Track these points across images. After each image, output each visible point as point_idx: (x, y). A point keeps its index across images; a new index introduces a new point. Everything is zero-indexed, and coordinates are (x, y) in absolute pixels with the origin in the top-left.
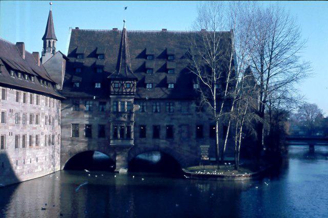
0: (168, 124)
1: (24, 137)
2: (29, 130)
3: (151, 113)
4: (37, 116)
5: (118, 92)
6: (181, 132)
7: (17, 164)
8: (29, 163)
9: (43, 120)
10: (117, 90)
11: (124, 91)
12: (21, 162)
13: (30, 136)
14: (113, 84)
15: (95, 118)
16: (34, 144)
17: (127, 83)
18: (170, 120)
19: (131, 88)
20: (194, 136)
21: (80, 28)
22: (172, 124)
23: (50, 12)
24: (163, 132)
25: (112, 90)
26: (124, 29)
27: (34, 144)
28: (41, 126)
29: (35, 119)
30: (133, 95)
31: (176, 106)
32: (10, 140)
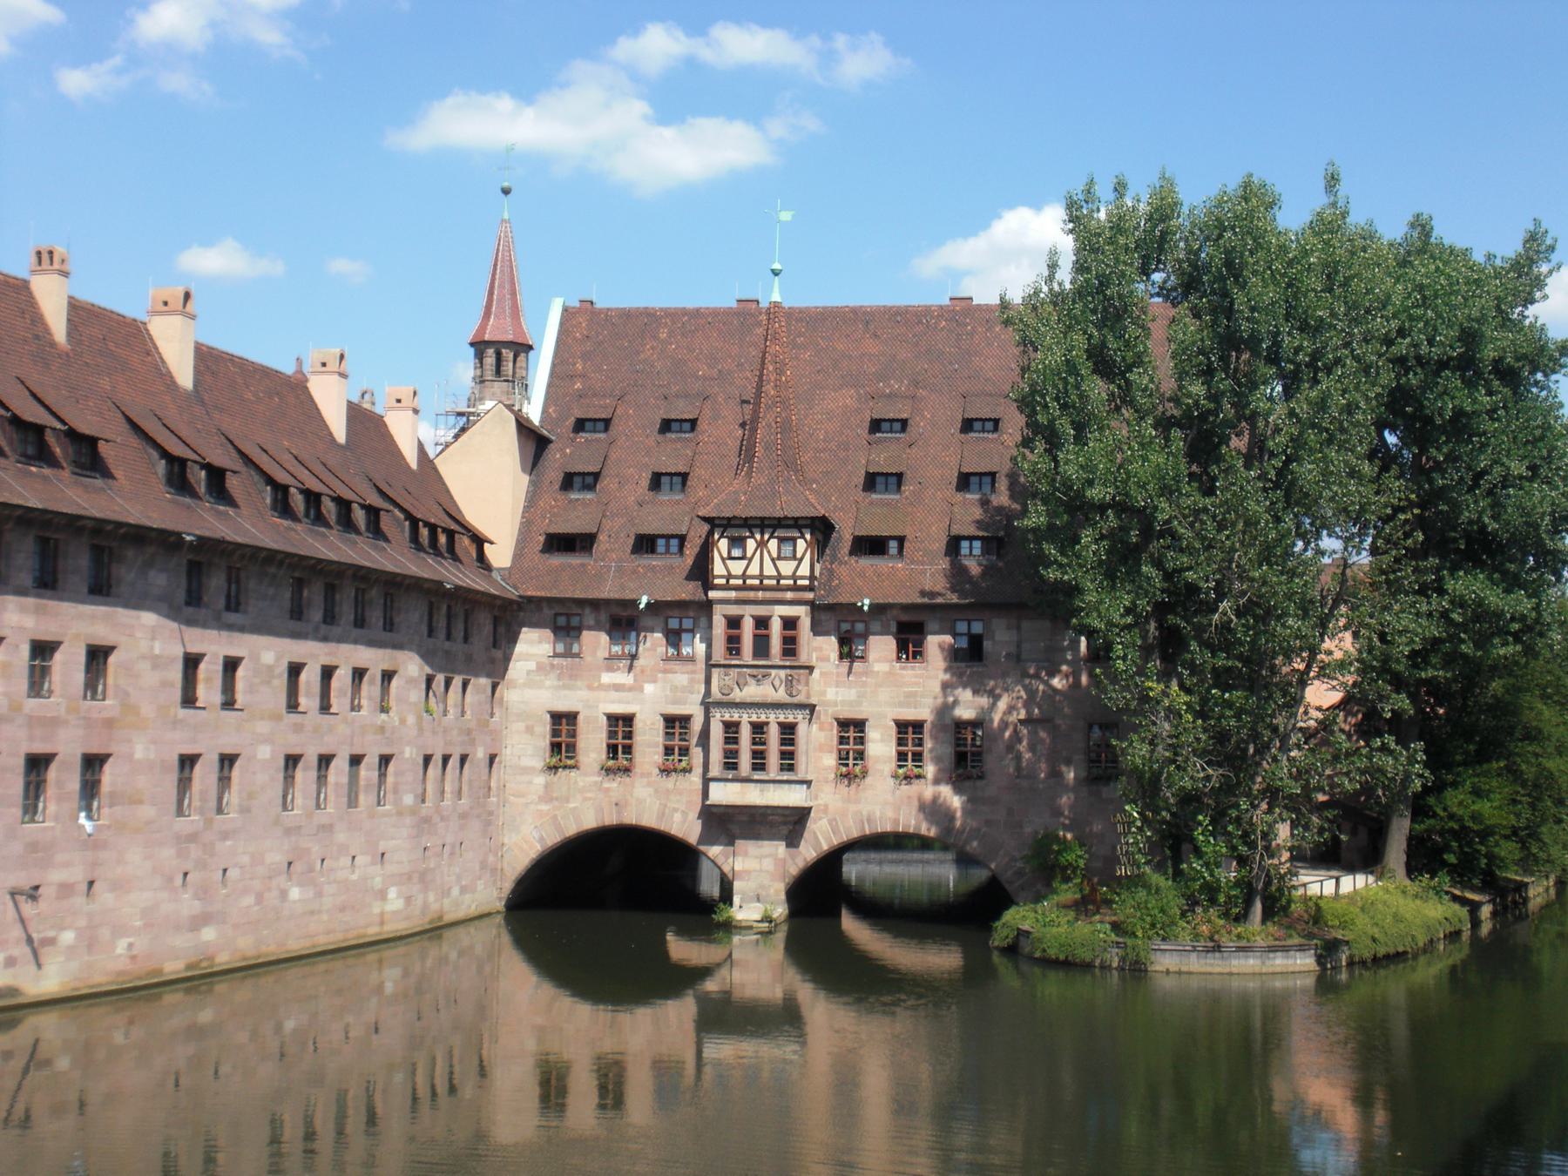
1: (325, 761)
5: (744, 576)
11: (769, 570)
12: (311, 870)
13: (356, 760)
14: (723, 544)
15: (649, 688)
19: (801, 560)
21: (600, 304)
25: (718, 568)
28: (403, 721)
30: (810, 588)
31: (998, 637)
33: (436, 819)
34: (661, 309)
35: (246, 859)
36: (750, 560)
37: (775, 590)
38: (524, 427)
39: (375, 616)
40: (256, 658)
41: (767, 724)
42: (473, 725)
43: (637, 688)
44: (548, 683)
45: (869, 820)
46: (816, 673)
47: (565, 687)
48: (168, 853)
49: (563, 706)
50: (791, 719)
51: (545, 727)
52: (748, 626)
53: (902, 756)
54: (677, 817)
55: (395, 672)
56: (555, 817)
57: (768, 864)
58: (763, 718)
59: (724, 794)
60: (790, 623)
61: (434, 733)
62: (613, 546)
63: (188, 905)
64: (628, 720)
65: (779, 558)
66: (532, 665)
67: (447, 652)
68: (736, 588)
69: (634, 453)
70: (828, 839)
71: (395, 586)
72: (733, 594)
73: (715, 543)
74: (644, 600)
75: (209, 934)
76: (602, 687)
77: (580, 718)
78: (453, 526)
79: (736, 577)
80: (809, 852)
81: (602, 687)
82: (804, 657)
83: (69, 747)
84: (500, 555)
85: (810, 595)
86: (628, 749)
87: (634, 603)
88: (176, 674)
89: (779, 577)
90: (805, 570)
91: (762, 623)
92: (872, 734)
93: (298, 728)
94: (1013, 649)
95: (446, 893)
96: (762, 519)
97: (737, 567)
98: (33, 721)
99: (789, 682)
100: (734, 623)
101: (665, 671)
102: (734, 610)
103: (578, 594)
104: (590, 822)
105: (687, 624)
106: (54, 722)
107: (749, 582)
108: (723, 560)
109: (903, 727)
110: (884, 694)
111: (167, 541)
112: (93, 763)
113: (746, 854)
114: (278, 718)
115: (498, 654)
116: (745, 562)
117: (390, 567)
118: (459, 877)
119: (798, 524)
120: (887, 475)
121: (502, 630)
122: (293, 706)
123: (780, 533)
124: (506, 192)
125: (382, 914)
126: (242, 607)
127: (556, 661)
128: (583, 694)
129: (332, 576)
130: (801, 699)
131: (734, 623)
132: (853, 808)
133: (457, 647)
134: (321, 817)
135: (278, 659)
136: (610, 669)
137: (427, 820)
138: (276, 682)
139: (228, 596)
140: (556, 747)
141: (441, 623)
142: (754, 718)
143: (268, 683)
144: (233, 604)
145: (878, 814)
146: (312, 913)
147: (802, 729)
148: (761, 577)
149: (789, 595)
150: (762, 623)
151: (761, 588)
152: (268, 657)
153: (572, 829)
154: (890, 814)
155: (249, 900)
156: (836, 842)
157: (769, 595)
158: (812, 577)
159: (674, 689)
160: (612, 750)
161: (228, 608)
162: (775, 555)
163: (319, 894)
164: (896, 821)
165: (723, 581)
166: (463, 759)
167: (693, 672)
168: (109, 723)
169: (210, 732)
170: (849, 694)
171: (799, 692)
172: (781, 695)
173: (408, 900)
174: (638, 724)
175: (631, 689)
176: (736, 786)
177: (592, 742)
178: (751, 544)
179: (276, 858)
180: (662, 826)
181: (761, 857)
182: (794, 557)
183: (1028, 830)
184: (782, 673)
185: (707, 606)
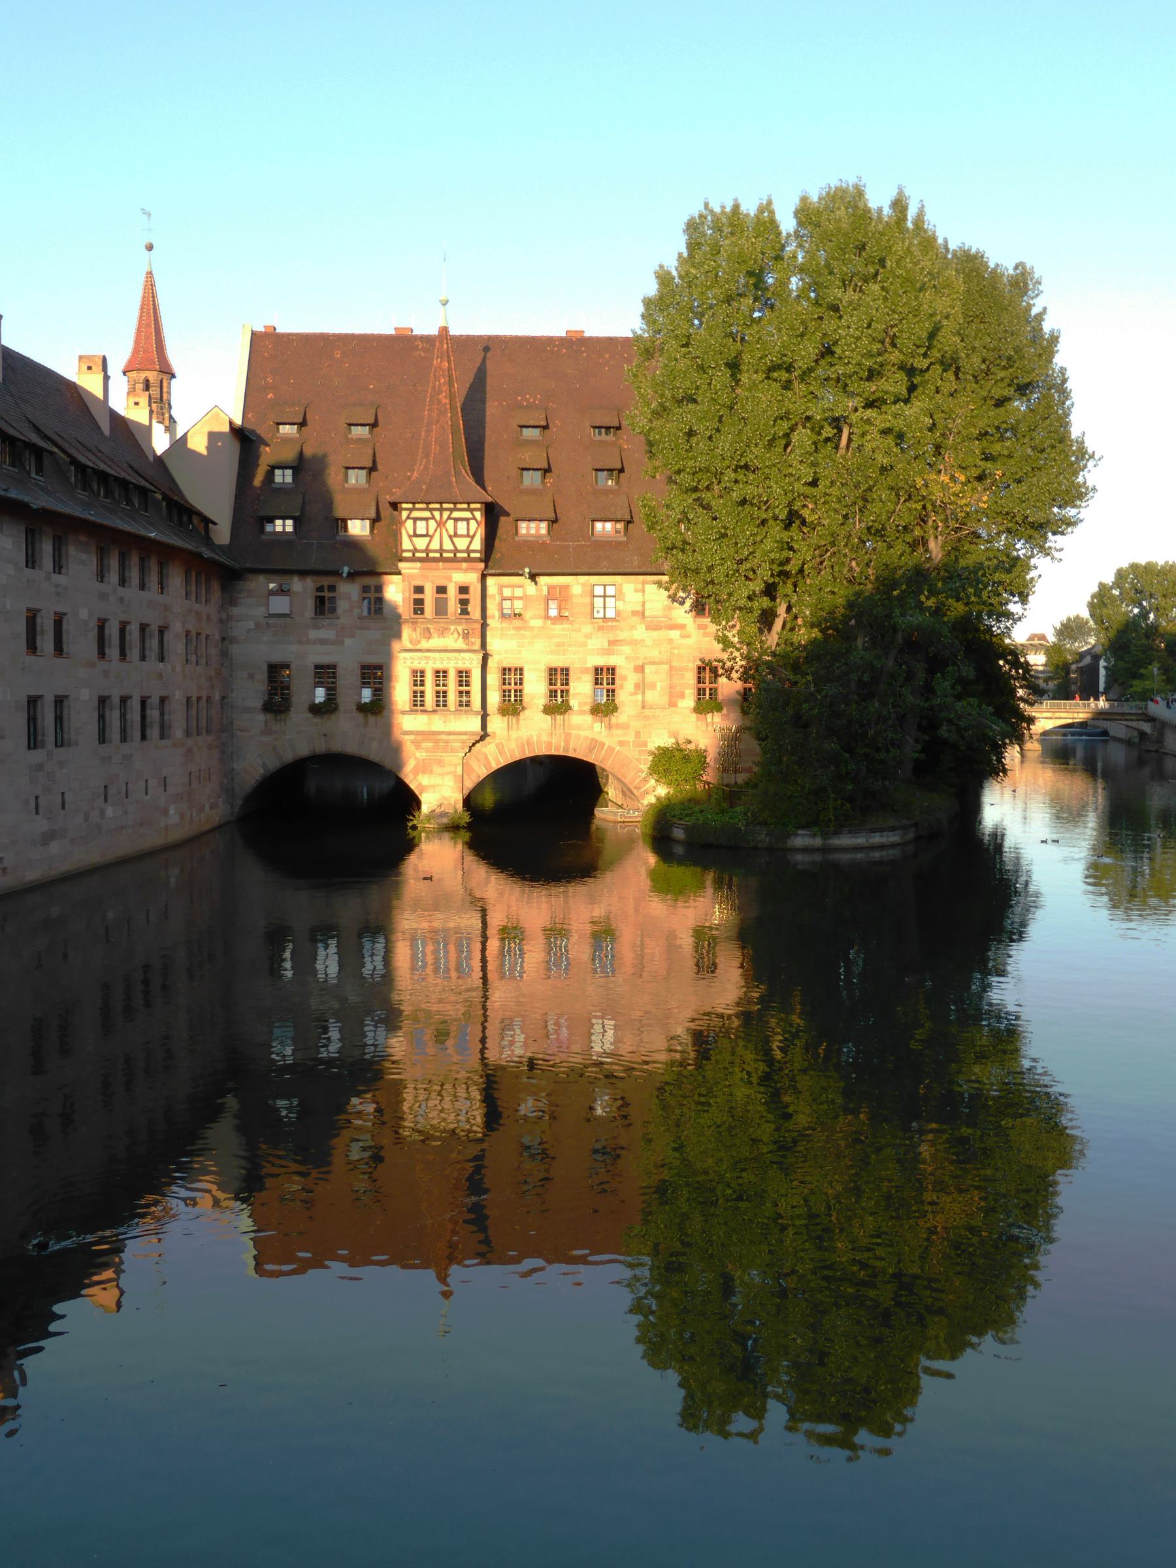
0: (601, 661)
1: (124, 700)
2: (133, 677)
3: (538, 623)
5: (427, 551)
6: (640, 687)
7: (106, 800)
10: (421, 543)
11: (448, 545)
13: (143, 703)
14: (409, 523)
15: (348, 642)
18: (606, 645)
19: (473, 537)
20: (689, 702)
21: (280, 330)
23: (150, 274)
24: (582, 689)
25: (406, 544)
26: (444, 330)
27: (153, 733)
28: (173, 670)
29: (154, 643)
30: (480, 560)
34: (334, 335)
36: (432, 537)
37: (454, 560)
39: (153, 580)
43: (339, 642)
44: (265, 638)
45: (528, 743)
49: (277, 658)
51: (262, 676)
53: (552, 694)
55: (166, 627)
63: (41, 825)
65: (456, 535)
66: (251, 625)
67: (197, 613)
68: (420, 560)
72: (418, 565)
73: (402, 523)
74: (346, 569)
75: (54, 847)
77: (293, 666)
81: (309, 642)
84: (222, 534)
88: (21, 627)
89: (456, 551)
90: (477, 544)
95: (202, 809)
97: (421, 543)
99: (466, 636)
100: (419, 589)
101: (361, 628)
104: (303, 750)
107: (431, 555)
108: (410, 537)
109: (552, 672)
110: (539, 645)
113: (431, 772)
114: (93, 665)
116: (428, 539)
117: (172, 542)
122: (102, 653)
123: (456, 514)
124: (150, 247)
125: (166, 828)
126: (63, 570)
127: (271, 621)
128: (294, 648)
132: (514, 734)
134: (125, 748)
136: (316, 627)
145: (535, 739)
148: (441, 551)
149: (464, 565)
150: (442, 590)
151: (442, 559)
152: (84, 614)
153: (289, 757)
154: (545, 738)
156: (503, 763)
162: (452, 533)
164: (549, 744)
165: (410, 554)
166: (209, 698)
169: (48, 676)
171: (473, 643)
173: (182, 815)
174: (340, 672)
175: (333, 643)
180: (363, 753)
181: (443, 775)
182: (468, 535)
183: (652, 746)
184: (460, 629)
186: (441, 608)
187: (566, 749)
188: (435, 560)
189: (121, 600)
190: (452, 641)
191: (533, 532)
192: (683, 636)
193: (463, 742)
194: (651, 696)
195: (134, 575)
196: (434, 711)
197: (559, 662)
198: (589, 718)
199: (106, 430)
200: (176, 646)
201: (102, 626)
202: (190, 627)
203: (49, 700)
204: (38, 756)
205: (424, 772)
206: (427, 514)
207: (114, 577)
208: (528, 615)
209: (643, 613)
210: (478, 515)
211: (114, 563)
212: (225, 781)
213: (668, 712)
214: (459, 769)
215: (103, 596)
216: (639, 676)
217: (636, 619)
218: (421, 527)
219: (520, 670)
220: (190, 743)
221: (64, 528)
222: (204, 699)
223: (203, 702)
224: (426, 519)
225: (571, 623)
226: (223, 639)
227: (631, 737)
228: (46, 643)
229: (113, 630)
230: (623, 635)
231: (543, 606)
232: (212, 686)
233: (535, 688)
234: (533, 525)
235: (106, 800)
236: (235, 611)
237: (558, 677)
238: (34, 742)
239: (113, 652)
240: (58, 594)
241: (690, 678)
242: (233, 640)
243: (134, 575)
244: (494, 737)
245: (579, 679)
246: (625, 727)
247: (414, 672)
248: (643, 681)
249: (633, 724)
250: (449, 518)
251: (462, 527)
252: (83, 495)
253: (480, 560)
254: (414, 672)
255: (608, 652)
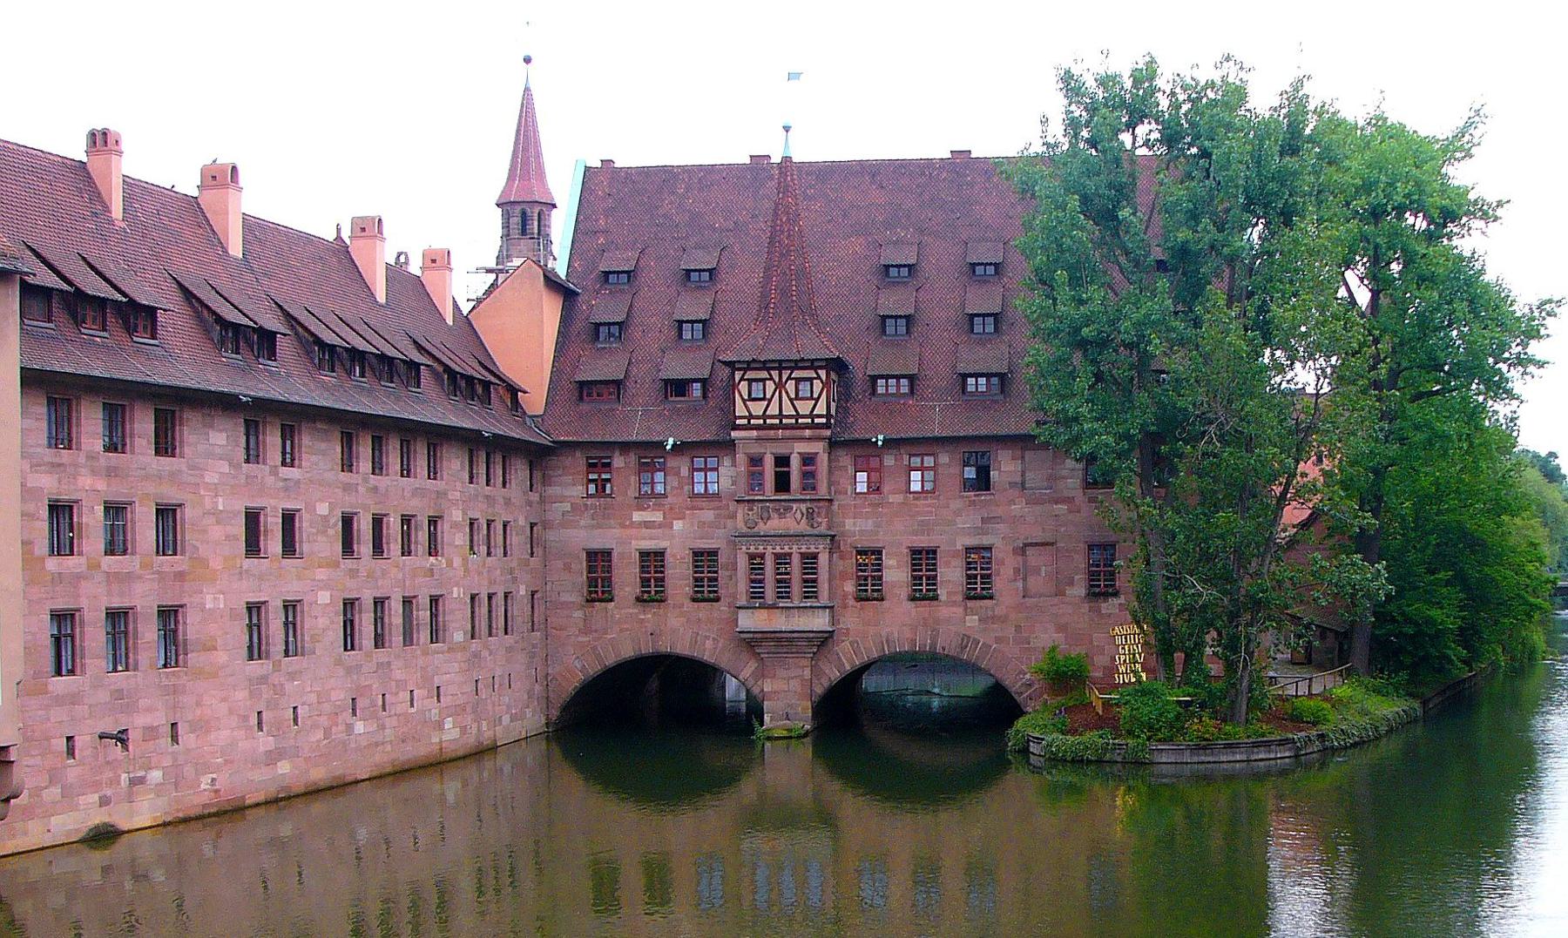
1: (379, 603)
2: (396, 575)
3: (899, 498)
4: (433, 522)
5: (764, 416)
6: (1023, 573)
7: (354, 714)
8: (404, 707)
9: (461, 539)
10: (757, 408)
11: (788, 410)
13: (407, 602)
14: (743, 386)
15: (678, 525)
16: (424, 635)
17: (798, 380)
20: (1079, 590)
22: (986, 541)
24: (951, 575)
25: (740, 410)
28: (450, 564)
29: (422, 536)
30: (827, 426)
32: (322, 622)
33: (485, 653)
35: (313, 698)
38: (552, 282)
40: (311, 508)
41: (790, 554)
42: (514, 564)
44: (582, 523)
46: (835, 506)
47: (599, 527)
48: (241, 694)
49: (597, 544)
50: (812, 550)
52: (769, 462)
53: (917, 579)
54: (709, 644)
55: (441, 517)
56: (594, 648)
57: (795, 685)
58: (786, 549)
59: (750, 621)
60: (808, 460)
61: (480, 574)
62: (642, 390)
63: (265, 742)
64: (660, 555)
65: (797, 398)
67: (487, 497)
68: (757, 428)
69: (658, 303)
70: (851, 661)
71: (438, 437)
72: (755, 433)
73: (734, 386)
74: (671, 441)
75: (284, 767)
76: (632, 525)
78: (493, 379)
79: (758, 417)
80: (832, 675)
82: (823, 491)
83: (144, 599)
84: (535, 400)
85: (828, 433)
86: (661, 581)
87: (661, 445)
88: (239, 529)
89: (798, 416)
90: (821, 409)
91: (782, 461)
92: (888, 561)
93: (353, 573)
94: (1019, 479)
96: (780, 362)
97: (757, 408)
98: (111, 577)
99: (810, 515)
100: (755, 461)
101: (693, 508)
102: (755, 449)
103: (608, 439)
104: (628, 652)
105: (712, 462)
106: (129, 577)
109: (916, 553)
111: (225, 404)
112: (169, 615)
114: (337, 565)
115: (534, 497)
118: (509, 707)
119: (813, 365)
120: (896, 317)
121: (538, 474)
122: (348, 547)
128: (617, 532)
129: (380, 428)
130: (823, 529)
131: (755, 461)
132: (872, 630)
133: (497, 491)
134: (381, 655)
135: (332, 508)
136: (641, 508)
137: (476, 655)
138: (331, 532)
139: (284, 453)
140: (592, 582)
141: (481, 470)
142: (778, 550)
143: (324, 532)
144: (289, 460)
146: (377, 744)
147: (823, 559)
148: (781, 416)
149: (807, 433)
150: (782, 461)
151: (781, 426)
152: (323, 509)
153: (611, 661)
155: (320, 735)
157: (788, 433)
158: (828, 416)
159: (702, 524)
160: (645, 582)
161: (284, 464)
163: (383, 727)
167: (718, 508)
168: (180, 576)
169: (274, 579)
170: (869, 524)
172: (803, 527)
173: (464, 730)
174: (669, 559)
175: (660, 526)
176: (764, 614)
177: (626, 579)
178: (770, 386)
179: (340, 696)
182: (811, 398)
184: (803, 507)
185: (730, 445)
186: (782, 483)
187: (933, 645)
188: (772, 427)
189: (375, 489)
190: (794, 522)
191: (892, 390)
192: (1070, 511)
193: (809, 640)
194: (1034, 583)
195: (393, 460)
196: (774, 607)
197: (923, 542)
198: (961, 610)
199: (381, 297)
200: (454, 538)
201: (347, 521)
202: (471, 514)
203: (276, 605)
204: (257, 667)
205: (763, 676)
206: (764, 374)
207: (365, 465)
208: (886, 489)
209: (1024, 488)
210: (823, 373)
211: (364, 449)
212: (537, 687)
213: (1056, 600)
214: (807, 672)
215: (347, 488)
216: (1020, 558)
217: (1015, 492)
218: (757, 390)
219: (880, 553)
220: (475, 645)
221: (294, 419)
222: (501, 595)
223: (499, 600)
224: (763, 380)
225: (937, 498)
226: (532, 526)
227: (1010, 632)
228: (273, 543)
229: (364, 526)
230: (999, 511)
231: (904, 479)
232: (515, 580)
233: (896, 573)
234: (892, 382)
235: (354, 714)
236: (553, 491)
237: (923, 559)
238: (255, 651)
239: (365, 547)
240: (286, 489)
241: (1080, 561)
242: (546, 525)
243: (393, 460)
244: (847, 633)
245: (948, 564)
246: (1003, 620)
247: (752, 557)
248: (1025, 562)
249: (1013, 616)
250: (789, 378)
251: (805, 388)
252: (328, 378)
253: (827, 426)
254: (752, 557)
255: (983, 532)
